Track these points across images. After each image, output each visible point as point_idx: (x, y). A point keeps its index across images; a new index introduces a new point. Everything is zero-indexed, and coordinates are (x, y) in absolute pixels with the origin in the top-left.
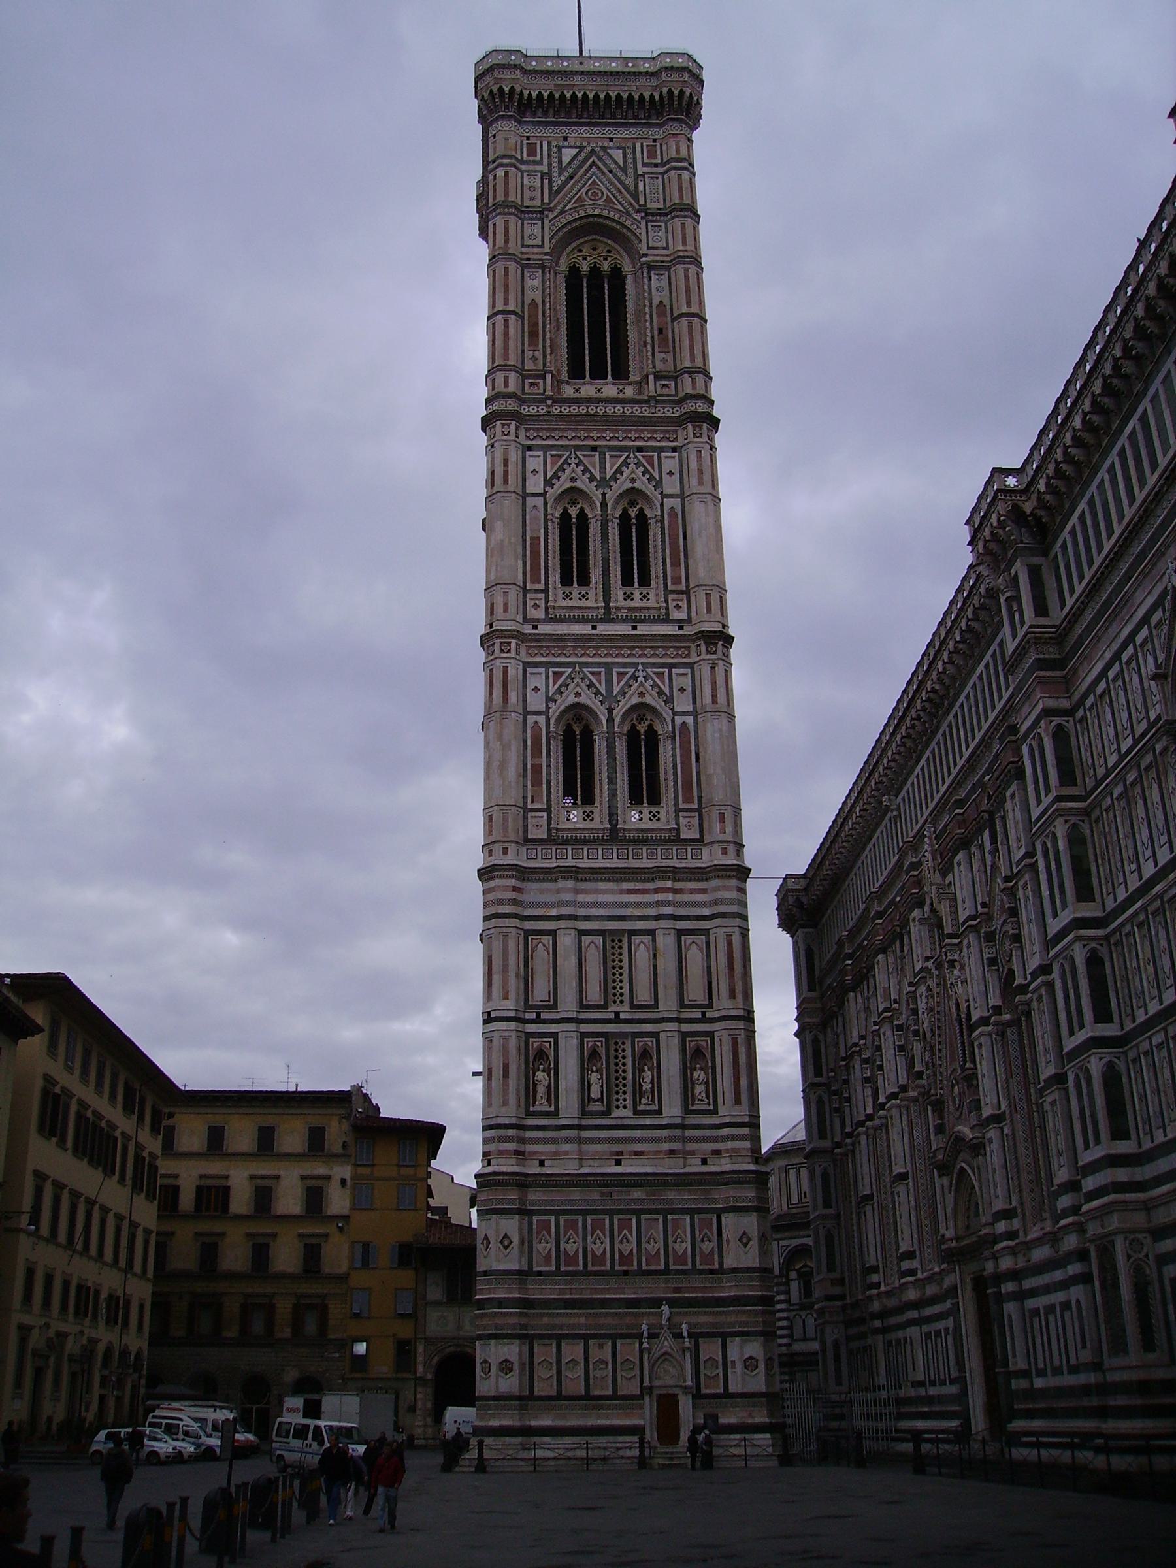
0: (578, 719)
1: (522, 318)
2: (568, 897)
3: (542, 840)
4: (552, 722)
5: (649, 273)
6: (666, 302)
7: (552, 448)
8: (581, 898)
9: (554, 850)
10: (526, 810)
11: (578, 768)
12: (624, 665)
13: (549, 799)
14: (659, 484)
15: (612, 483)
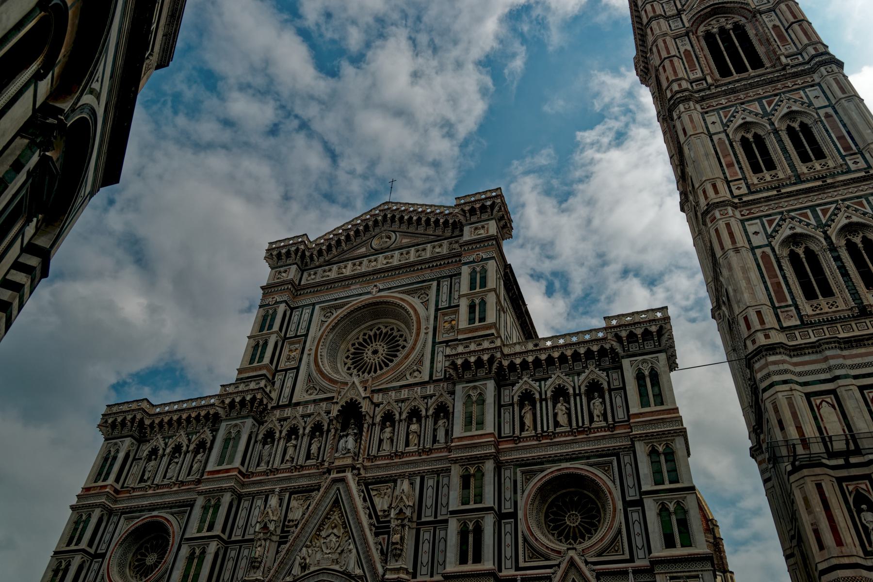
0: (798, 245)
1: (682, 59)
2: (840, 361)
3: (796, 327)
4: (776, 249)
5: (760, 15)
6: (778, 23)
7: (722, 109)
8: (849, 362)
9: (810, 331)
10: (774, 308)
11: (810, 275)
12: (825, 204)
13: (793, 299)
14: (810, 104)
15: (773, 112)
